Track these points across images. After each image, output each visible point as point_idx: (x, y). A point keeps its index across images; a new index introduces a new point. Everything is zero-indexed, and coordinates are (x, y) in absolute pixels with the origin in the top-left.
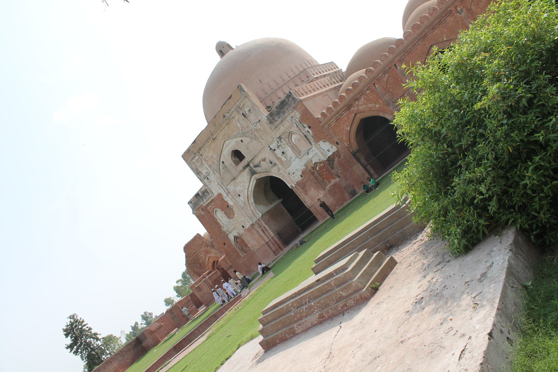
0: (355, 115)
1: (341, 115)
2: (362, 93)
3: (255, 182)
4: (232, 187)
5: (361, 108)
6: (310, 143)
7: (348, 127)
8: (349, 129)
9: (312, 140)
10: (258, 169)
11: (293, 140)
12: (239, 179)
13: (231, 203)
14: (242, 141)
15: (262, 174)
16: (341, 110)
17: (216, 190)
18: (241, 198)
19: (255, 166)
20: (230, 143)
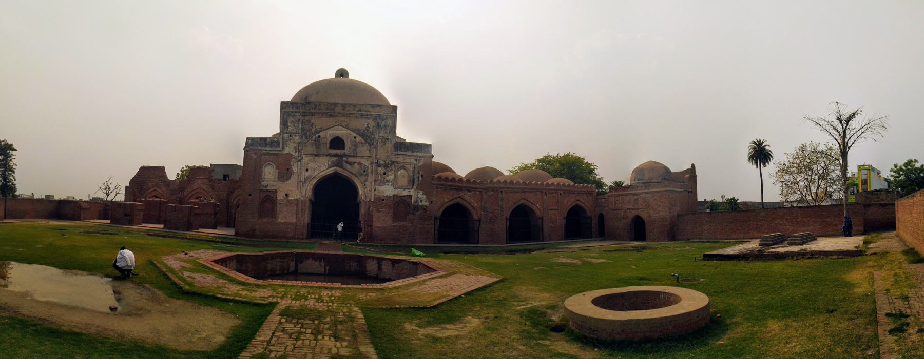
2: (474, 190)
5: (466, 197)
7: (446, 199)
9: (415, 185)
10: (348, 167)
12: (321, 159)
13: (295, 169)
17: (289, 149)
18: (307, 174)
19: (347, 162)
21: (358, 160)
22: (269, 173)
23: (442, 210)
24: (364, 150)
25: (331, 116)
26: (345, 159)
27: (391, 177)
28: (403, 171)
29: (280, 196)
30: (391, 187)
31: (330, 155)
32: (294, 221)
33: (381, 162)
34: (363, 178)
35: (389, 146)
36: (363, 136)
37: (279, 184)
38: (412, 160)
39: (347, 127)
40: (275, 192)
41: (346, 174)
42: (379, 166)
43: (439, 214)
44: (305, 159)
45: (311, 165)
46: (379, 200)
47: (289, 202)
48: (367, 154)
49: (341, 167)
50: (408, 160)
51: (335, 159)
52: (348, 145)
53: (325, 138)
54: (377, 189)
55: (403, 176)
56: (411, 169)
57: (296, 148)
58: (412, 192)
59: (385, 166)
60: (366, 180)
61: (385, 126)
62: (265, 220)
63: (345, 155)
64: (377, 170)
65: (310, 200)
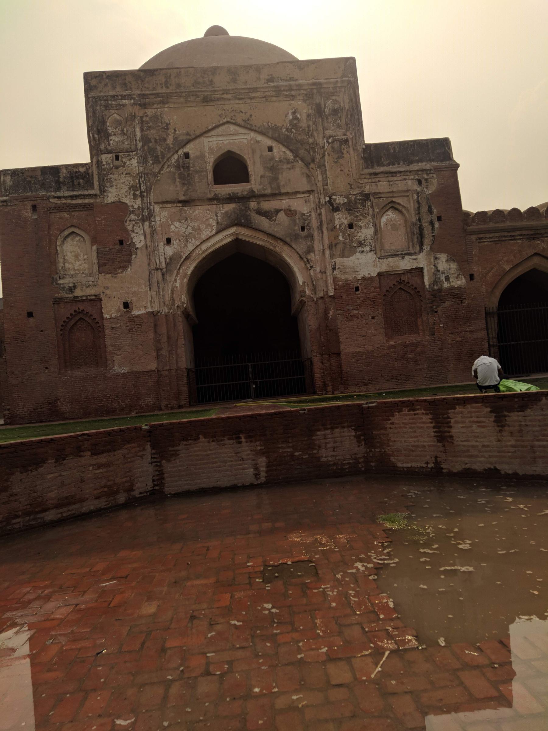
0: (536, 254)
1: (513, 238)
3: (229, 240)
4: (165, 214)
6: (421, 244)
8: (507, 268)
9: (427, 241)
10: (264, 223)
11: (384, 219)
12: (199, 211)
13: (138, 240)
14: (270, 149)
15: (260, 236)
16: (521, 229)
17: (118, 191)
19: (260, 212)
20: (238, 134)
21: (284, 203)
22: (76, 257)
23: (498, 293)
24: (294, 177)
25: (207, 100)
26: (253, 204)
27: (366, 232)
28: (390, 216)
29: (111, 310)
30: (371, 256)
31: (217, 200)
32: (153, 366)
33: (340, 200)
34: (301, 247)
35: (352, 158)
36: (285, 141)
37: (104, 280)
38: (411, 184)
39: (248, 126)
40: (96, 300)
41: (260, 240)
42: (336, 209)
43: (494, 302)
44: (161, 215)
45: (176, 227)
46: (348, 291)
47: (136, 321)
48: (303, 185)
49: (248, 225)
50: (400, 185)
51: (230, 207)
52: (256, 169)
53: (202, 157)
54: (340, 262)
55: (395, 227)
56: (412, 206)
57: (133, 188)
58: (422, 260)
59: (350, 207)
60: (310, 250)
61: (335, 112)
62: (78, 373)
63: (252, 196)
64: (331, 220)
65: (186, 315)
